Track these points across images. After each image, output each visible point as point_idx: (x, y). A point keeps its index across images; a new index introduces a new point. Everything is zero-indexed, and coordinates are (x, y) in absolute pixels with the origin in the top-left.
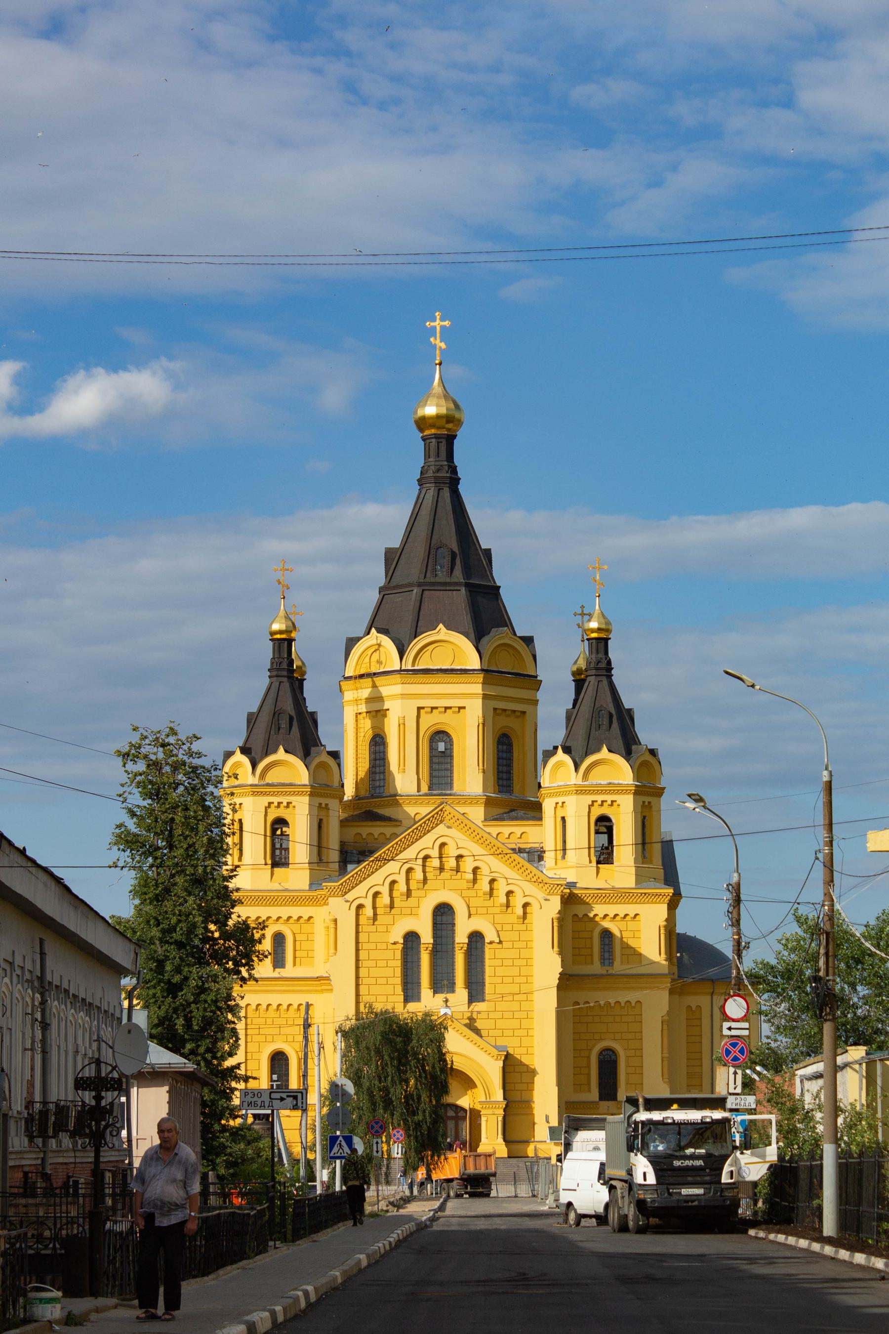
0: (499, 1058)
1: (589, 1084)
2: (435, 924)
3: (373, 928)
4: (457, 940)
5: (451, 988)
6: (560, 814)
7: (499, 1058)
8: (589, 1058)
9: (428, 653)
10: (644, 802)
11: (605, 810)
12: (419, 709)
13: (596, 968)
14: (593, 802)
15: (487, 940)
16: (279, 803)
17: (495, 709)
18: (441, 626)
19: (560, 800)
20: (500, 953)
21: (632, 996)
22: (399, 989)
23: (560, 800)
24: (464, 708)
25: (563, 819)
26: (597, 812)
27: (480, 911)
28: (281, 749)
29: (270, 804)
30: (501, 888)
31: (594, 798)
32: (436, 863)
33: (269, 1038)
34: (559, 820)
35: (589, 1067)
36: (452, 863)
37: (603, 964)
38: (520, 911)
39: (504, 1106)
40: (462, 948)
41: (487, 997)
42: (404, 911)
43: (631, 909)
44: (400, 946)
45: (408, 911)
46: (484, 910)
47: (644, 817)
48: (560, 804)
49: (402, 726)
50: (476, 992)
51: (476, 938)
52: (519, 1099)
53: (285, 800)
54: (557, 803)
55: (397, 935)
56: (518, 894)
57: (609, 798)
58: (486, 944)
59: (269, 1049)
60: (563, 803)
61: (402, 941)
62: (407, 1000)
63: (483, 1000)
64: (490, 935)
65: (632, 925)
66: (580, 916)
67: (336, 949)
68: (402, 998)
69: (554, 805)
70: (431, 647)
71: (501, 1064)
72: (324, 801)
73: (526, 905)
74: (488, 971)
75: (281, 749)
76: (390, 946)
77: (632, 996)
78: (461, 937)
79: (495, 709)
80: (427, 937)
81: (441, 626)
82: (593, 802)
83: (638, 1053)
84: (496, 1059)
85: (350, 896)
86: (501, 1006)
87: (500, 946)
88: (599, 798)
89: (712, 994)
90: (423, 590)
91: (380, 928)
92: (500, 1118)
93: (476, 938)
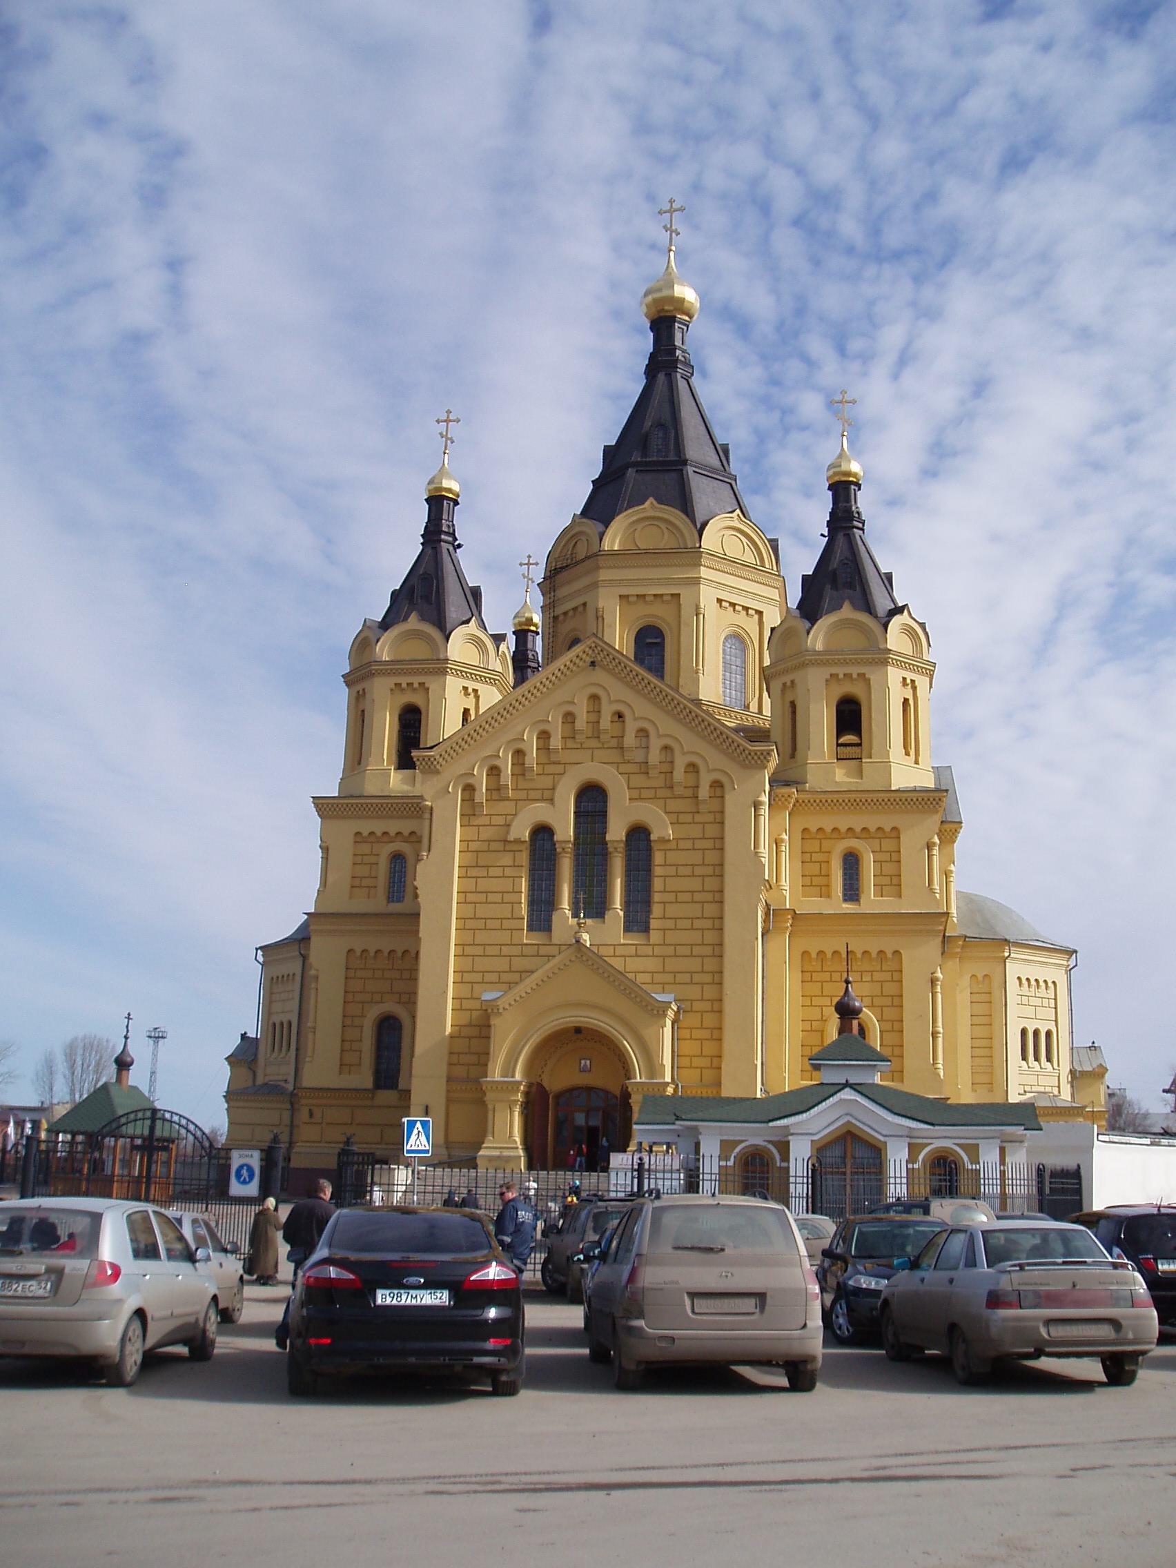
4: (608, 838)
6: (789, 699)
10: (904, 679)
14: (831, 675)
15: (653, 837)
17: (720, 601)
18: (651, 500)
19: (787, 679)
21: (889, 945)
23: (787, 679)
24: (679, 595)
25: (793, 705)
28: (413, 618)
29: (398, 685)
31: (834, 670)
33: (377, 997)
34: (788, 705)
41: (654, 924)
43: (887, 822)
47: (906, 701)
48: (789, 684)
49: (600, 619)
51: (639, 835)
53: (416, 680)
54: (784, 684)
58: (652, 844)
59: (374, 1013)
65: (888, 845)
69: (781, 686)
70: (640, 526)
72: (471, 685)
73: (717, 785)
74: (657, 884)
75: (413, 618)
78: (616, 831)
79: (720, 601)
80: (566, 830)
81: (651, 500)
82: (831, 675)
86: (671, 937)
88: (841, 671)
90: (637, 471)
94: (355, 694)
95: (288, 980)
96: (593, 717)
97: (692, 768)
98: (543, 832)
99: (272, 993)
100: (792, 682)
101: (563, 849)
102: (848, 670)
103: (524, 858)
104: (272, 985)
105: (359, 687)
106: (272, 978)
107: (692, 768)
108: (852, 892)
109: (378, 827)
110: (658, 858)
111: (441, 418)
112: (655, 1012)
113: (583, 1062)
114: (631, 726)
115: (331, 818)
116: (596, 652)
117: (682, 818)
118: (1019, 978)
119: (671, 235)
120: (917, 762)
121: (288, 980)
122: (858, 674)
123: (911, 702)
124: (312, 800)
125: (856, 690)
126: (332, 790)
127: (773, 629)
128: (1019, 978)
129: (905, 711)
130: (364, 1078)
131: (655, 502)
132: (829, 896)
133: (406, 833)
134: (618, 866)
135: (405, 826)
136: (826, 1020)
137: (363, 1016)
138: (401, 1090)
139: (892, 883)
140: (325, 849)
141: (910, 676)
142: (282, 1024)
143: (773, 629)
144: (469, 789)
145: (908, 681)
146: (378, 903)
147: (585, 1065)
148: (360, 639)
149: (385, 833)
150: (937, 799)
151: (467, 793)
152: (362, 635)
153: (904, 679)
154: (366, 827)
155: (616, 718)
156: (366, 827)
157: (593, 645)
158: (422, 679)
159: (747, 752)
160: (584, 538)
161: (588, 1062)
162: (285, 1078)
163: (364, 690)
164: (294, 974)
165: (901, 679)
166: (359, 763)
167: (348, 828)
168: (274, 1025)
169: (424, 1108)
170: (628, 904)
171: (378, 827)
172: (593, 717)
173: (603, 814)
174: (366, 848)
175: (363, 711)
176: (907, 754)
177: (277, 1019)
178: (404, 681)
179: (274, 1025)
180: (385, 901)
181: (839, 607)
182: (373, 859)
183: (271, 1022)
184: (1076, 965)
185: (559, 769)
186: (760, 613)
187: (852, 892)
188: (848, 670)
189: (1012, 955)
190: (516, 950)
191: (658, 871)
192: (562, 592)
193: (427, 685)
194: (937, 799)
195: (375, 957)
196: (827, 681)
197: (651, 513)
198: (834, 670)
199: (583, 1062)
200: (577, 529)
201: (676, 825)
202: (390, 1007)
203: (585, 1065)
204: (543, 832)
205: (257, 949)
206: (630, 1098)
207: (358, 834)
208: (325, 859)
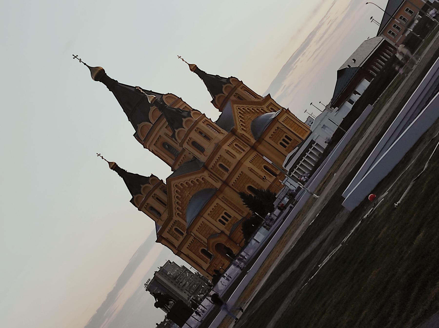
11: (191, 141)
12: (154, 145)
13: (226, 175)
26: (190, 143)
57: (188, 138)
77: (239, 172)
83: (253, 182)
108: (227, 170)
120: (212, 139)
139: (229, 164)
141: (195, 128)
146: (181, 238)
153: (195, 130)
156: (167, 230)
187: (227, 170)
195: (191, 245)
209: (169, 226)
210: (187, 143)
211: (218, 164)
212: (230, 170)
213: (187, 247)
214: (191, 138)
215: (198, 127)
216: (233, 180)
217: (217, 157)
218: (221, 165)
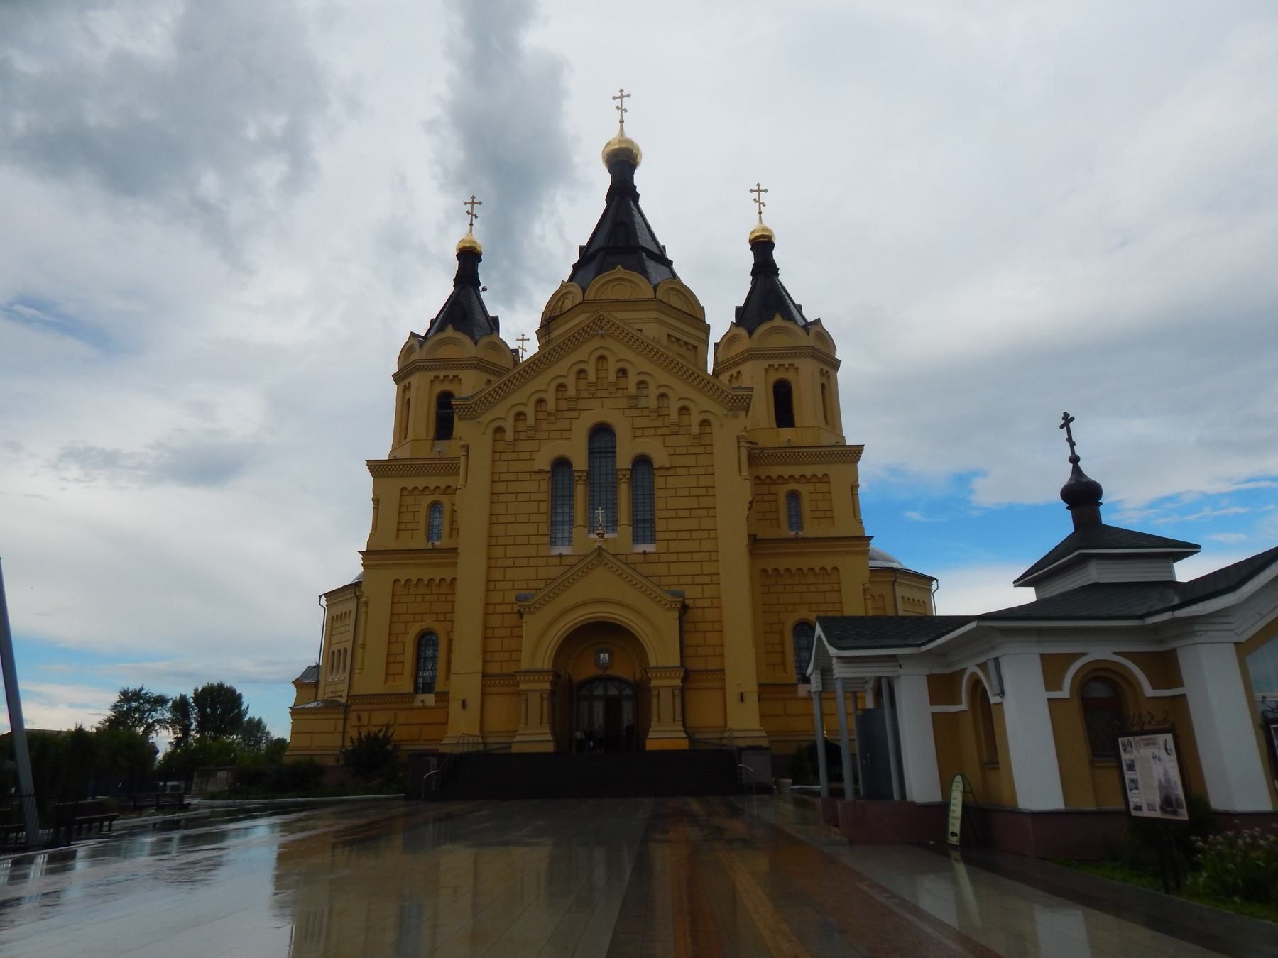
0: (673, 606)
1: (784, 663)
2: (592, 452)
3: (513, 456)
5: (613, 523)
7: (673, 606)
8: (782, 633)
9: (609, 289)
10: (822, 369)
16: (446, 377)
17: (669, 336)
18: (619, 267)
20: (672, 482)
21: (829, 563)
22: (544, 529)
23: (734, 372)
26: (774, 377)
27: (647, 432)
30: (674, 405)
32: (592, 377)
35: (782, 644)
36: (612, 377)
37: (791, 528)
38: (695, 429)
39: (682, 674)
40: (624, 476)
41: (659, 536)
42: (553, 435)
43: (819, 470)
44: (546, 477)
45: (558, 435)
46: (652, 432)
47: (823, 386)
48: (735, 375)
50: (644, 527)
52: (703, 668)
53: (451, 374)
54: (732, 376)
55: (543, 461)
56: (694, 411)
57: (786, 362)
59: (415, 629)
60: (739, 373)
61: (548, 469)
62: (553, 543)
63: (653, 540)
64: (659, 458)
65: (821, 487)
66: (764, 477)
67: (466, 482)
68: (546, 539)
69: (729, 378)
70: (611, 285)
71: (676, 614)
73: (705, 423)
74: (660, 504)
76: (534, 477)
77: (829, 563)
78: (624, 461)
79: (669, 336)
80: (580, 462)
81: (619, 267)
82: (769, 365)
84: (668, 609)
85: (486, 418)
87: (672, 472)
88: (776, 362)
89: (895, 581)
91: (522, 456)
92: (677, 692)
93: (642, 461)
94: (403, 387)
95: (345, 617)
96: (602, 374)
97: (684, 410)
98: (562, 464)
99: (332, 629)
100: (739, 373)
101: (580, 477)
102: (782, 362)
103: (545, 486)
104: (333, 622)
105: (406, 382)
106: (333, 617)
107: (684, 410)
109: (421, 482)
110: (659, 482)
111: (468, 202)
112: (669, 606)
113: (602, 655)
114: (633, 379)
115: (382, 476)
116: (604, 322)
117: (679, 450)
118: (903, 597)
119: (622, 113)
121: (345, 617)
122: (789, 365)
123: (826, 386)
124: (366, 463)
125: (790, 376)
126: (383, 454)
127: (716, 344)
128: (903, 597)
129: (823, 393)
130: (406, 685)
131: (622, 269)
132: (779, 527)
133: (443, 487)
134: (624, 491)
135: (443, 482)
136: (783, 624)
137: (406, 633)
138: (438, 693)
140: (376, 501)
141: (826, 368)
142: (339, 651)
143: (716, 344)
144: (500, 430)
145: (824, 371)
146: (420, 542)
147: (604, 658)
148: (406, 348)
149: (426, 488)
150: (857, 452)
151: (498, 436)
152: (409, 345)
154: (410, 483)
155: (621, 375)
156: (410, 483)
157: (601, 318)
158: (455, 373)
159: (730, 396)
160: (569, 296)
161: (606, 655)
162: (340, 694)
163: (410, 383)
164: (350, 612)
165: (819, 370)
166: (405, 438)
167: (396, 484)
168: (333, 653)
169: (461, 701)
170: (635, 522)
171: (421, 482)
172: (602, 374)
173: (612, 451)
174: (409, 500)
175: (409, 400)
176: (827, 423)
177: (335, 648)
178: (442, 374)
179: (333, 653)
180: (426, 540)
181: (771, 318)
182: (416, 508)
183: (331, 650)
184: (938, 588)
185: (575, 414)
186: (695, 348)
187: (796, 520)
188: (782, 362)
189: (897, 580)
190: (542, 562)
191: (658, 493)
192: (554, 334)
193: (459, 377)
194: (857, 452)
196: (766, 370)
197: (619, 276)
198: (771, 362)
199: (602, 655)
200: (564, 291)
201: (673, 456)
202: (429, 623)
203: (604, 658)
204: (562, 464)
205: (320, 597)
206: (650, 683)
207: (404, 488)
208: (376, 509)
209: (432, 482)
210: (767, 367)
211: (793, 486)
212: (809, 531)
213: (396, 581)
214: (797, 369)
215: (830, 373)
216: (782, 564)
217: (809, 470)
218: (794, 496)
